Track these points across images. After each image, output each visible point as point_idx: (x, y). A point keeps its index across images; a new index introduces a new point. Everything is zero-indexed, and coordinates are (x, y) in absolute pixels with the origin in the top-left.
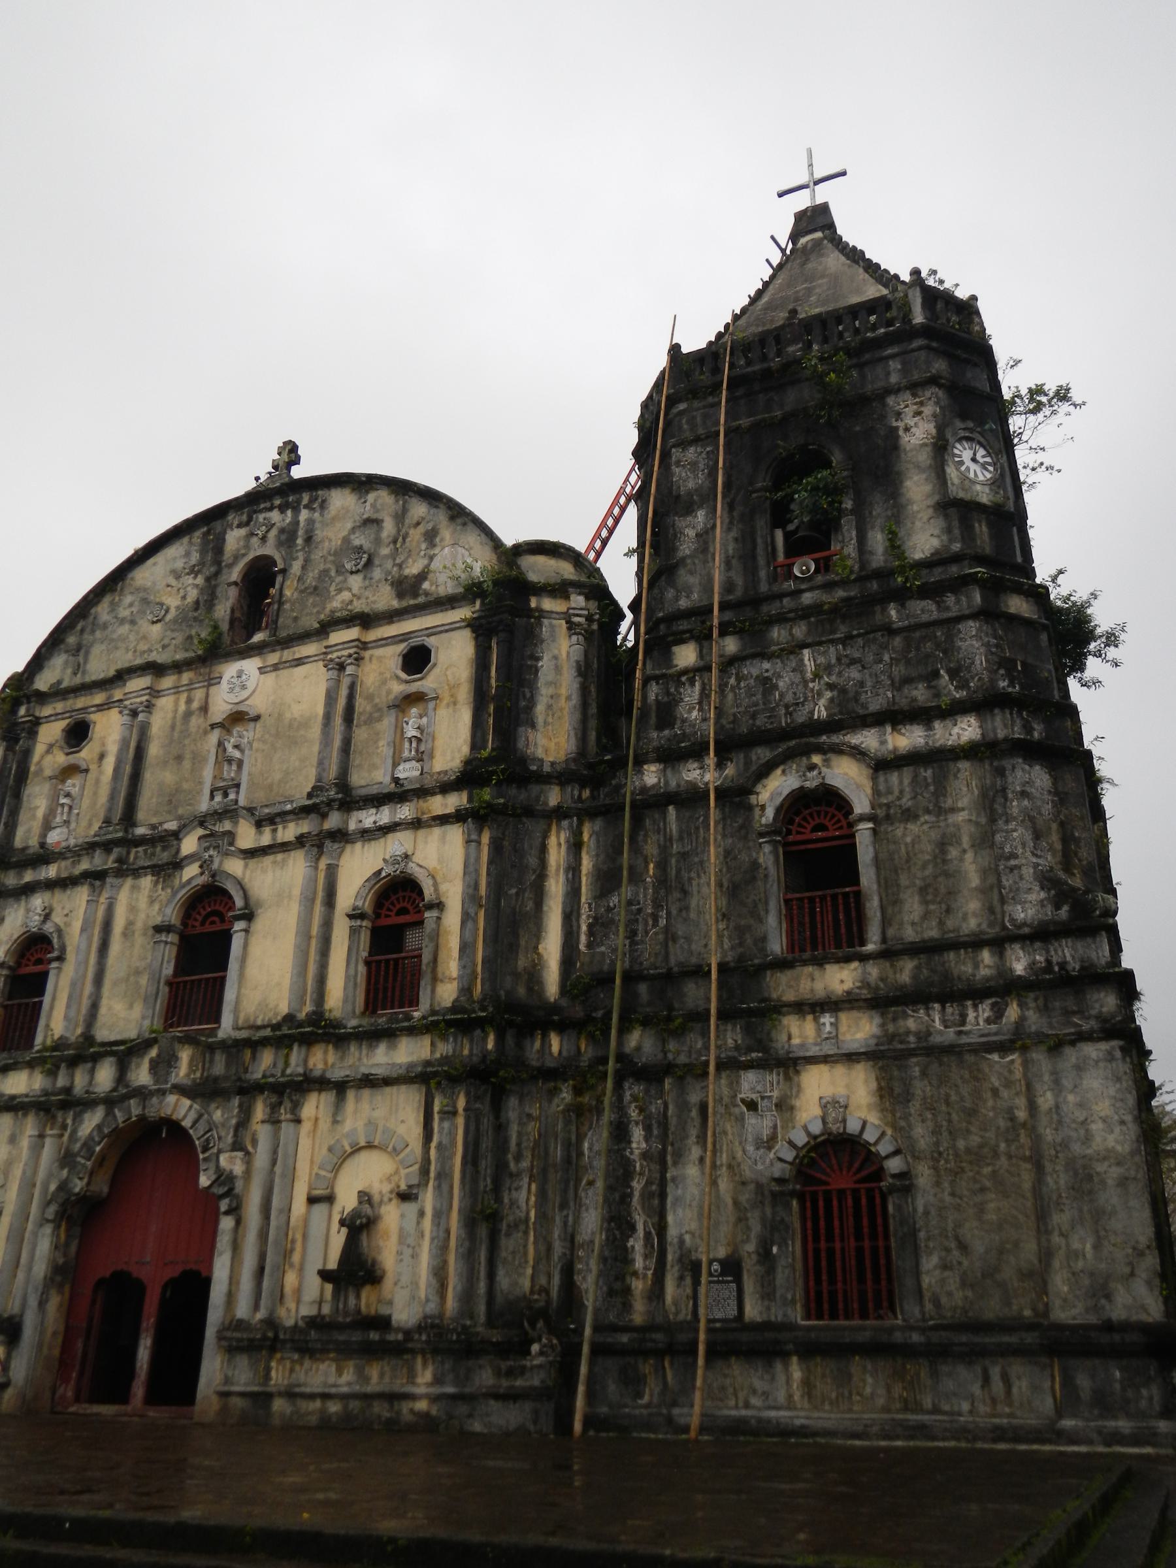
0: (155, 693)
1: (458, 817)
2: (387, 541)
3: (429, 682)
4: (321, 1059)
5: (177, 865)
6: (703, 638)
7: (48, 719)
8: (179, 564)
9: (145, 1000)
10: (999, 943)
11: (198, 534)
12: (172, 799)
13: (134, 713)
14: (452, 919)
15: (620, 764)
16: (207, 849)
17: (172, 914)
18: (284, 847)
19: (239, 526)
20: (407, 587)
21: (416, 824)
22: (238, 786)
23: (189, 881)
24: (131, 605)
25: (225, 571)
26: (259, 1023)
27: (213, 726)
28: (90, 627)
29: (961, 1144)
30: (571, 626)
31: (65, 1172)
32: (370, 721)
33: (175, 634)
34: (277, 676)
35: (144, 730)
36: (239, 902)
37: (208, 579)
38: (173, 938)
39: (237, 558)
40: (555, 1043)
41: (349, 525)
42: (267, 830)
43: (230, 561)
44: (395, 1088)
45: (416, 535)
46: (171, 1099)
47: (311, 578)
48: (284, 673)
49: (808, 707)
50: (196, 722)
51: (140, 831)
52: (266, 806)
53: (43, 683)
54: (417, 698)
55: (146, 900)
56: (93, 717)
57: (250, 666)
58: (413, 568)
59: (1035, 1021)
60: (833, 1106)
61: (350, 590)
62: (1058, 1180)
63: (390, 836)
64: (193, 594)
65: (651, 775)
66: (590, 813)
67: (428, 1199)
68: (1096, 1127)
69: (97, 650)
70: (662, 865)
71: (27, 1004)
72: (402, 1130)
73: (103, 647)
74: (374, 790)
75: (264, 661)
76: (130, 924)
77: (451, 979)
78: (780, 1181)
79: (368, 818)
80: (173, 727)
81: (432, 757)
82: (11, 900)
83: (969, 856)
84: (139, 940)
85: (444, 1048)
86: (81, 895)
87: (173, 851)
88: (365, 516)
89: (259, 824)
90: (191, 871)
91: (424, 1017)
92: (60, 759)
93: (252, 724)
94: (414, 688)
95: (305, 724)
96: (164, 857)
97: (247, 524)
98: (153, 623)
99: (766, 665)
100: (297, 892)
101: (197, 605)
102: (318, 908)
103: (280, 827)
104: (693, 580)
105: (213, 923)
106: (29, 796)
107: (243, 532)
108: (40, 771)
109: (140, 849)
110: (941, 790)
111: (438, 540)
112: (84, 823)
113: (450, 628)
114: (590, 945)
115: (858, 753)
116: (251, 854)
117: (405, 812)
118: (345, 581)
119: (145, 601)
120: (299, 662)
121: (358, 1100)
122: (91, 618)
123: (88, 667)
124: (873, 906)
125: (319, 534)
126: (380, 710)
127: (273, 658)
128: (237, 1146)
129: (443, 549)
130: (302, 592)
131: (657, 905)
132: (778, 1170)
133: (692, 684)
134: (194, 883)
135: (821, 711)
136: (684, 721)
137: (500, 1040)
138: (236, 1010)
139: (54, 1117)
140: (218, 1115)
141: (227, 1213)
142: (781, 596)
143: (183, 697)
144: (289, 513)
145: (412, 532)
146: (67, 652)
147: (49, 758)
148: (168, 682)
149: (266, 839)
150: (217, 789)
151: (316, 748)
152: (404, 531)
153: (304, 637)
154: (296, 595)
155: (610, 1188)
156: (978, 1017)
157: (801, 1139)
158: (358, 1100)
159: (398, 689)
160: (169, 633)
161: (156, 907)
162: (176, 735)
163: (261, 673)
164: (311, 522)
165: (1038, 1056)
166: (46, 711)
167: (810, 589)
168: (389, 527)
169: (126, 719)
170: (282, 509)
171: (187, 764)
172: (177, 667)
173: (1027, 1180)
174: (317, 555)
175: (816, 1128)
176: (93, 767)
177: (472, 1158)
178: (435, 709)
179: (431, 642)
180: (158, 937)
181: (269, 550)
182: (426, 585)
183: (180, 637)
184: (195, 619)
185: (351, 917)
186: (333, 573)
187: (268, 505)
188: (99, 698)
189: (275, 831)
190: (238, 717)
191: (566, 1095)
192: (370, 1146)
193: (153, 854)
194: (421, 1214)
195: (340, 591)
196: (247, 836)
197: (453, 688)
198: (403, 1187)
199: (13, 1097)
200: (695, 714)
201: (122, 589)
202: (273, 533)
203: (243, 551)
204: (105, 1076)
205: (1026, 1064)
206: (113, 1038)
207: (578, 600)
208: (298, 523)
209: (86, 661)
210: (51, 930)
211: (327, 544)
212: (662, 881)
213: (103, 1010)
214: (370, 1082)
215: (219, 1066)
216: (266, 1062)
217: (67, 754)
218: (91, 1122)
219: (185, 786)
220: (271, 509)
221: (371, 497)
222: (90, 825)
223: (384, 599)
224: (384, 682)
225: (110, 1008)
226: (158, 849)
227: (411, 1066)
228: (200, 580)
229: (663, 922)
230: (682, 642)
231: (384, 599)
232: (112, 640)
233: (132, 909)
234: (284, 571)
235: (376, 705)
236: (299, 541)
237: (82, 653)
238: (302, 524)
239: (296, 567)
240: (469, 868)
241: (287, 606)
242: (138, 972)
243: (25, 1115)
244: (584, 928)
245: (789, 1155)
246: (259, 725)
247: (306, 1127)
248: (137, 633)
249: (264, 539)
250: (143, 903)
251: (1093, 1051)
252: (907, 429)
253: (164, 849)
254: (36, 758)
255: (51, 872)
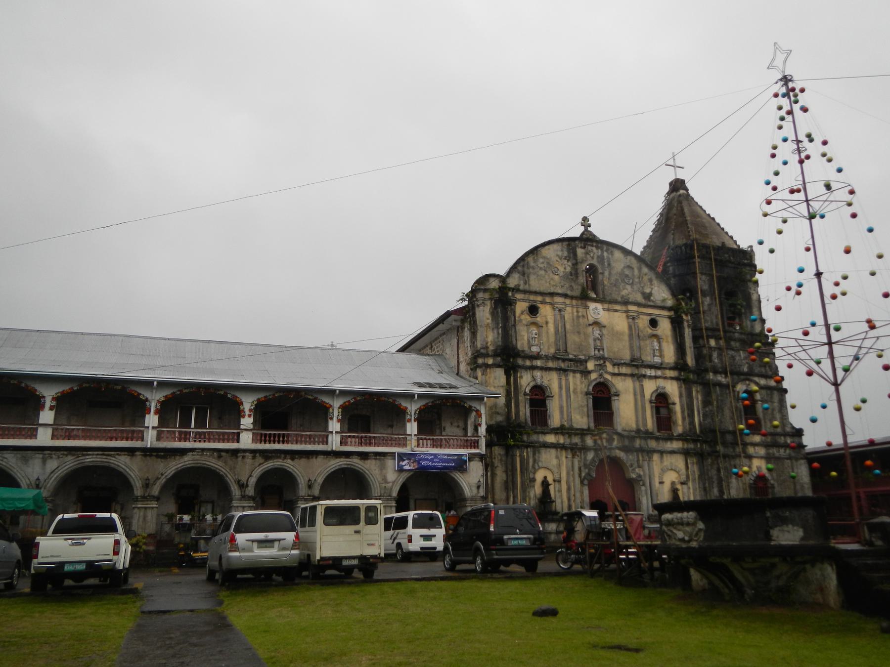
0: (566, 305)
1: (676, 379)
2: (637, 277)
3: (659, 331)
4: (653, 444)
5: (589, 372)
6: (718, 339)
7: (519, 300)
8: (560, 253)
9: (588, 416)
10: (785, 435)
11: (565, 243)
12: (580, 347)
13: (560, 310)
14: (678, 408)
15: (706, 371)
16: (600, 370)
17: (591, 388)
18: (625, 375)
19: (581, 247)
20: (648, 296)
21: (665, 378)
22: (603, 349)
23: (596, 379)
24: (543, 263)
25: (579, 264)
26: (627, 429)
27: (590, 325)
28: (526, 266)
29: (782, 478)
30: (689, 326)
31: (587, 470)
32: (643, 340)
33: (566, 283)
34: (609, 313)
35: (563, 317)
36: (613, 391)
37: (573, 265)
38: (591, 397)
39: (583, 261)
40: (704, 445)
41: (622, 265)
42: (616, 367)
43: (581, 260)
44: (676, 455)
45: (646, 278)
46: (617, 451)
47: (613, 279)
48: (611, 313)
49: (743, 367)
50: (581, 320)
51: (571, 356)
52: (615, 359)
53: (512, 282)
54: (655, 336)
55: (579, 382)
56: (539, 305)
57: (599, 306)
58: (647, 291)
59: (793, 454)
60: (759, 468)
61: (627, 289)
62: (798, 487)
63: (657, 379)
64: (568, 269)
65: (711, 376)
66: (701, 384)
67: (690, 484)
68: (804, 477)
69: (532, 277)
70: (717, 402)
71: (538, 410)
72: (680, 466)
73: (535, 277)
74: (649, 363)
75: (603, 306)
76: (575, 390)
77: (680, 426)
78: (751, 484)
79: (649, 372)
80: (573, 319)
81: (664, 357)
82: (523, 371)
83: (778, 414)
84: (580, 396)
85: (686, 446)
86: (554, 376)
87: (585, 367)
88: (628, 264)
89: (614, 365)
90: (594, 376)
91: (677, 436)
92: (526, 318)
93: (603, 328)
94: (655, 332)
95: (622, 334)
96: (582, 368)
97: (584, 248)
98: (556, 275)
99: (733, 352)
100: (631, 390)
101: (571, 274)
102: (639, 397)
103: (620, 367)
104: (708, 318)
105: (600, 394)
106: (519, 330)
107: (583, 251)
108: (520, 321)
109: (572, 363)
110: (772, 394)
111: (653, 283)
112: (546, 348)
113: (663, 316)
114: (704, 420)
115: (757, 384)
116: (614, 374)
117: (659, 373)
118: (625, 286)
119: (548, 263)
120: (616, 311)
121: (667, 457)
122: (526, 262)
123: (531, 283)
124: (763, 422)
125: (613, 264)
126: (645, 337)
127: (606, 306)
128: (639, 467)
129: (655, 287)
130: (611, 284)
131: (718, 413)
132: (751, 482)
133: (715, 351)
134: (598, 380)
135: (746, 369)
136: (714, 362)
137: (701, 445)
138: (620, 425)
139: (576, 452)
140: (631, 457)
141: (642, 485)
142: (730, 332)
143: (575, 310)
144: (600, 251)
145: (644, 277)
146: (519, 273)
147: (523, 317)
148: (568, 301)
149: (616, 371)
150: (597, 348)
151: (628, 344)
152: (641, 275)
153: (615, 302)
154: (608, 285)
155: (718, 483)
156: (782, 451)
157: (755, 475)
158: (667, 457)
159: (650, 331)
160: (562, 281)
161: (584, 385)
162: (576, 324)
163: (603, 310)
164: (608, 258)
165: (794, 461)
166: (519, 296)
167: (738, 333)
168: (636, 272)
169: (557, 312)
170: (597, 248)
171: (582, 336)
172: (572, 298)
173: (792, 487)
174: (614, 272)
175: (757, 472)
176: (544, 326)
177: (700, 477)
178: (663, 342)
179: (658, 318)
180: (588, 396)
181: (595, 262)
182: (652, 298)
183: (567, 285)
184: (572, 279)
185: (651, 402)
186: (620, 281)
187: (591, 244)
188: (539, 298)
189: (619, 368)
190: (596, 323)
191: (710, 460)
192: (672, 469)
193: (577, 366)
194: (689, 488)
195: (624, 289)
196: (610, 368)
197: (667, 337)
198: (682, 481)
199: (552, 443)
200: (716, 361)
201: (537, 255)
202: (595, 257)
203: (585, 259)
204: (589, 441)
205: (792, 463)
206: (578, 427)
207: (689, 318)
208: (604, 256)
209: (529, 280)
210: (546, 386)
211: (616, 269)
212: (718, 407)
213: (573, 417)
214: (673, 452)
215: (627, 443)
216: (638, 443)
217: (532, 317)
218: (590, 456)
219: (583, 344)
220: (592, 246)
221: (629, 257)
222: (549, 349)
223: (639, 298)
224: (645, 328)
225: (575, 417)
226: (579, 364)
227: (679, 449)
228: (570, 263)
229: (719, 417)
230: (712, 338)
231: (639, 298)
232: (538, 275)
233: (575, 384)
234: (602, 273)
235: (644, 335)
236: (606, 264)
237: (526, 276)
238: (605, 257)
239: (607, 273)
240: (681, 396)
241: (606, 287)
242: (582, 406)
243: (561, 450)
244: (701, 415)
245: (753, 478)
246: (606, 329)
247: (654, 463)
248: (549, 276)
249: (593, 258)
250: (578, 383)
251: (802, 461)
252: (753, 294)
253: (581, 365)
254: (517, 314)
255: (539, 363)
